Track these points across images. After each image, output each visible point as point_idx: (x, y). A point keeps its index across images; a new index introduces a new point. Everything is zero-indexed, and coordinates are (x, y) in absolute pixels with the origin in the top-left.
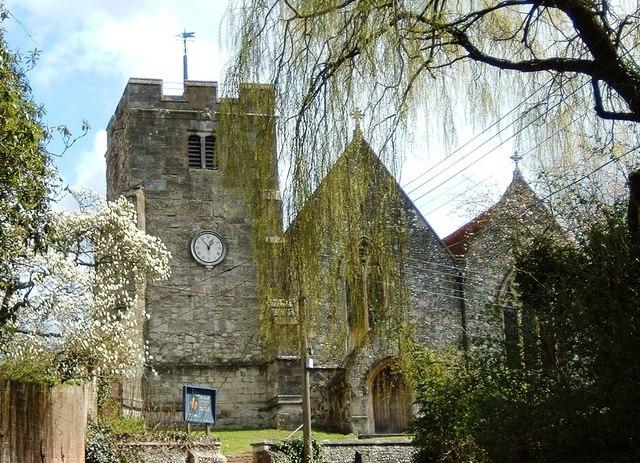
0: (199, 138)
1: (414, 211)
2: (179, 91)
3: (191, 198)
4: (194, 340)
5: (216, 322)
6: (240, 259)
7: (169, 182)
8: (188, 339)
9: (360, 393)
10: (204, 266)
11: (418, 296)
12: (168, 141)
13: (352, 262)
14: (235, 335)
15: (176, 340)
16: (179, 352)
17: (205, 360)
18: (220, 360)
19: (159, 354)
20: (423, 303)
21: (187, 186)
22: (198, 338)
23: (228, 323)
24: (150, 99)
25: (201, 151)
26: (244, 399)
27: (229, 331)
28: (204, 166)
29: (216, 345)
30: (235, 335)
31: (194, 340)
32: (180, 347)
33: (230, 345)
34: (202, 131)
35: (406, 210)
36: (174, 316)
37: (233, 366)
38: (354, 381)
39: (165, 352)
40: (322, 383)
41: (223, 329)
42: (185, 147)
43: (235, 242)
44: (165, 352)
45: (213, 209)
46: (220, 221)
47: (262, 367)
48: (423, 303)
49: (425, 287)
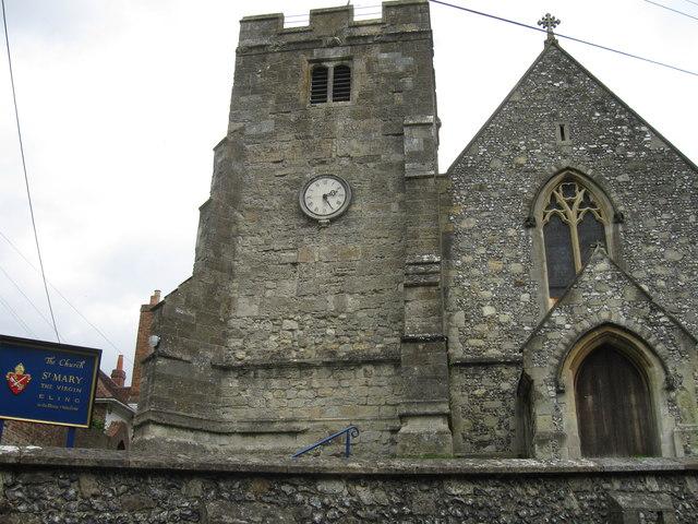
0: (326, 69)
1: (644, 129)
2: (304, 22)
3: (307, 137)
4: (295, 325)
5: (331, 298)
6: (373, 208)
7: (277, 122)
8: (288, 324)
9: (551, 391)
10: (317, 221)
11: (663, 244)
12: (282, 75)
13: (554, 202)
14: (360, 315)
15: (269, 327)
16: (272, 343)
17: (311, 355)
18: (333, 353)
19: (243, 349)
20: (671, 255)
21: (301, 124)
22: (302, 325)
23: (349, 299)
24: (265, 34)
25: (331, 82)
26: (367, 413)
27: (350, 310)
28: (330, 99)
29: (329, 331)
30: (360, 315)
31: (295, 325)
32: (273, 338)
33: (350, 332)
34: (329, 60)
35: (632, 127)
36: (269, 293)
37: (353, 362)
38: (541, 375)
39: (251, 345)
40: (505, 386)
41: (341, 309)
42: (305, 79)
43: (367, 185)
44: (251, 345)
45: (338, 147)
46: (345, 162)
47: (395, 362)
48: (671, 255)
49: (674, 230)
